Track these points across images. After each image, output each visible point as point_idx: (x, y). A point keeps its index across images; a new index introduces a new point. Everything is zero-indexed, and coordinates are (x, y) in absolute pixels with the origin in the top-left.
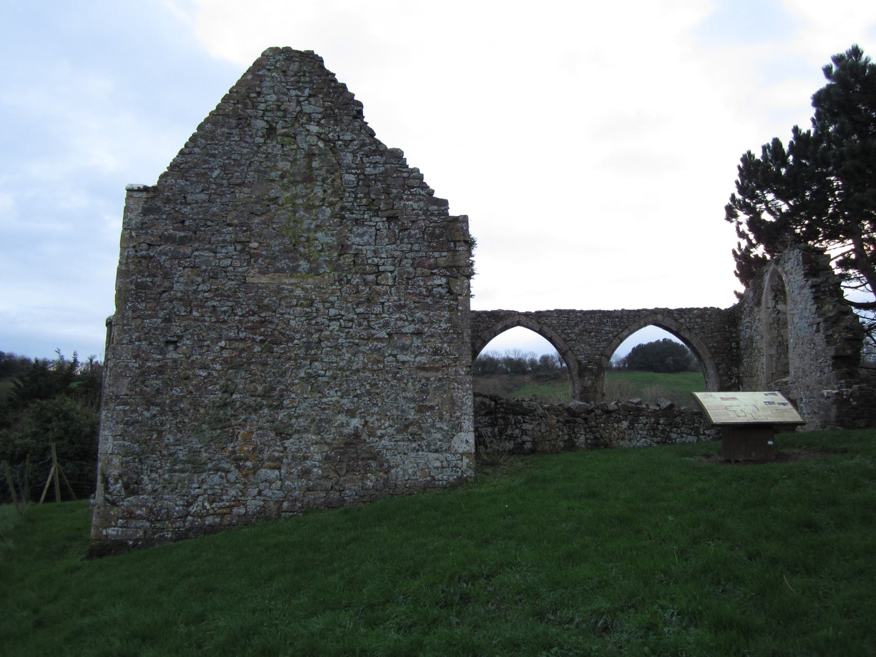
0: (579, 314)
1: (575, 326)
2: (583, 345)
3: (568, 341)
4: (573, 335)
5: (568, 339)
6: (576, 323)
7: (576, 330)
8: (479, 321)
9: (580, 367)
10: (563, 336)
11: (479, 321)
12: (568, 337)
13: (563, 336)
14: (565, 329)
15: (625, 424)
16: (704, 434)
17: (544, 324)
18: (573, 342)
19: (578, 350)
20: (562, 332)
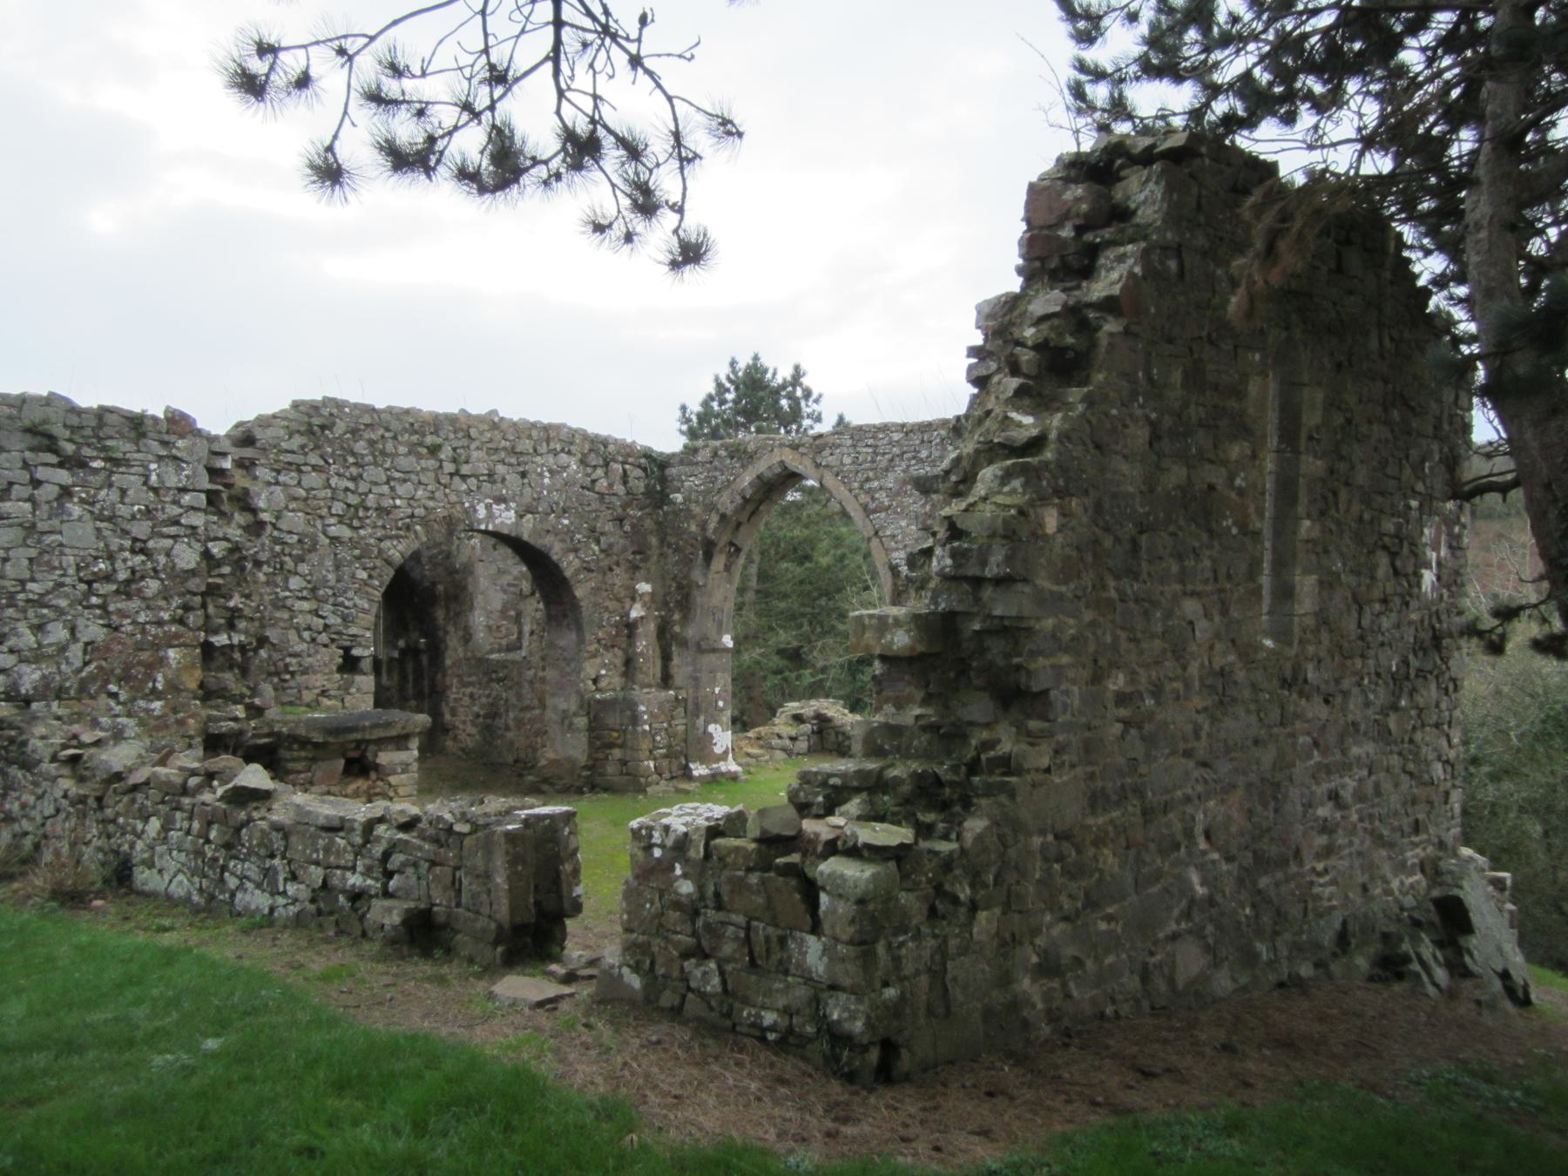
0: (896, 436)
1: (887, 470)
2: (903, 523)
3: (875, 511)
4: (882, 497)
5: (872, 506)
6: (892, 460)
7: (890, 481)
8: (716, 469)
9: (895, 584)
10: (863, 498)
11: (716, 469)
12: (873, 499)
13: (863, 498)
14: (868, 480)
15: (155, 824)
16: (284, 893)
17: (827, 466)
18: (883, 515)
19: (893, 536)
20: (861, 488)
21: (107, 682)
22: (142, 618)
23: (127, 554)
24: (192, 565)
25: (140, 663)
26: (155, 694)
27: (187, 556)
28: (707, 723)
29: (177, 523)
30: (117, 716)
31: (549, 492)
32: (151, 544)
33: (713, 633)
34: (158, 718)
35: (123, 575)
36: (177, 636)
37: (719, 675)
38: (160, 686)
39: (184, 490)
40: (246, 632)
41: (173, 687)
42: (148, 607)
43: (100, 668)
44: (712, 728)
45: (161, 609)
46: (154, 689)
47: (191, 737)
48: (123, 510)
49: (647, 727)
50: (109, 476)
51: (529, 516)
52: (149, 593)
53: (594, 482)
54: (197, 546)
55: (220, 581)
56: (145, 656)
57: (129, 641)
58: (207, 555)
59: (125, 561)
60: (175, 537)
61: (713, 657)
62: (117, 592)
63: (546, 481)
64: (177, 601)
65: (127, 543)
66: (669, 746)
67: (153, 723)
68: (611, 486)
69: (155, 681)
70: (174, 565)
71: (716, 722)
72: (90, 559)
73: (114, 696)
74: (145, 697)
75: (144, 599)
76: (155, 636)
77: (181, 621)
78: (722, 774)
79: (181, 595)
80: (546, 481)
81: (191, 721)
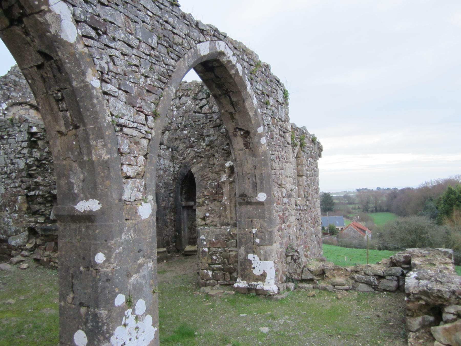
21: (6, 207)
22: (12, 186)
23: (10, 165)
24: (23, 167)
25: (12, 201)
26: (15, 212)
27: (21, 164)
28: (247, 253)
29: (21, 153)
30: (8, 218)
31: (177, 118)
32: (14, 161)
33: (249, 191)
34: (17, 220)
35: (8, 172)
36: (20, 192)
37: (255, 221)
38: (17, 209)
39: (22, 141)
40: (42, 191)
41: (20, 209)
42: (13, 182)
43: (3, 202)
44: (250, 256)
45: (17, 183)
46: (15, 210)
47: (25, 228)
48: (10, 151)
49: (206, 249)
50: (8, 140)
51: (167, 132)
52: (13, 177)
53: (201, 108)
54: (24, 160)
55: (33, 172)
56: (13, 198)
57: (9, 194)
58: (27, 164)
59: (9, 167)
60: (19, 158)
61: (250, 208)
62: (7, 177)
63: (175, 113)
64: (20, 179)
65: (10, 161)
66: (223, 263)
67: (15, 221)
68: (211, 108)
69: (16, 207)
70: (19, 167)
71: (254, 253)
72: (3, 167)
73: (7, 211)
74: (14, 212)
75: (12, 179)
76: (14, 192)
77: (20, 186)
78: (257, 290)
79: (21, 178)
80: (175, 113)
81: (24, 222)
